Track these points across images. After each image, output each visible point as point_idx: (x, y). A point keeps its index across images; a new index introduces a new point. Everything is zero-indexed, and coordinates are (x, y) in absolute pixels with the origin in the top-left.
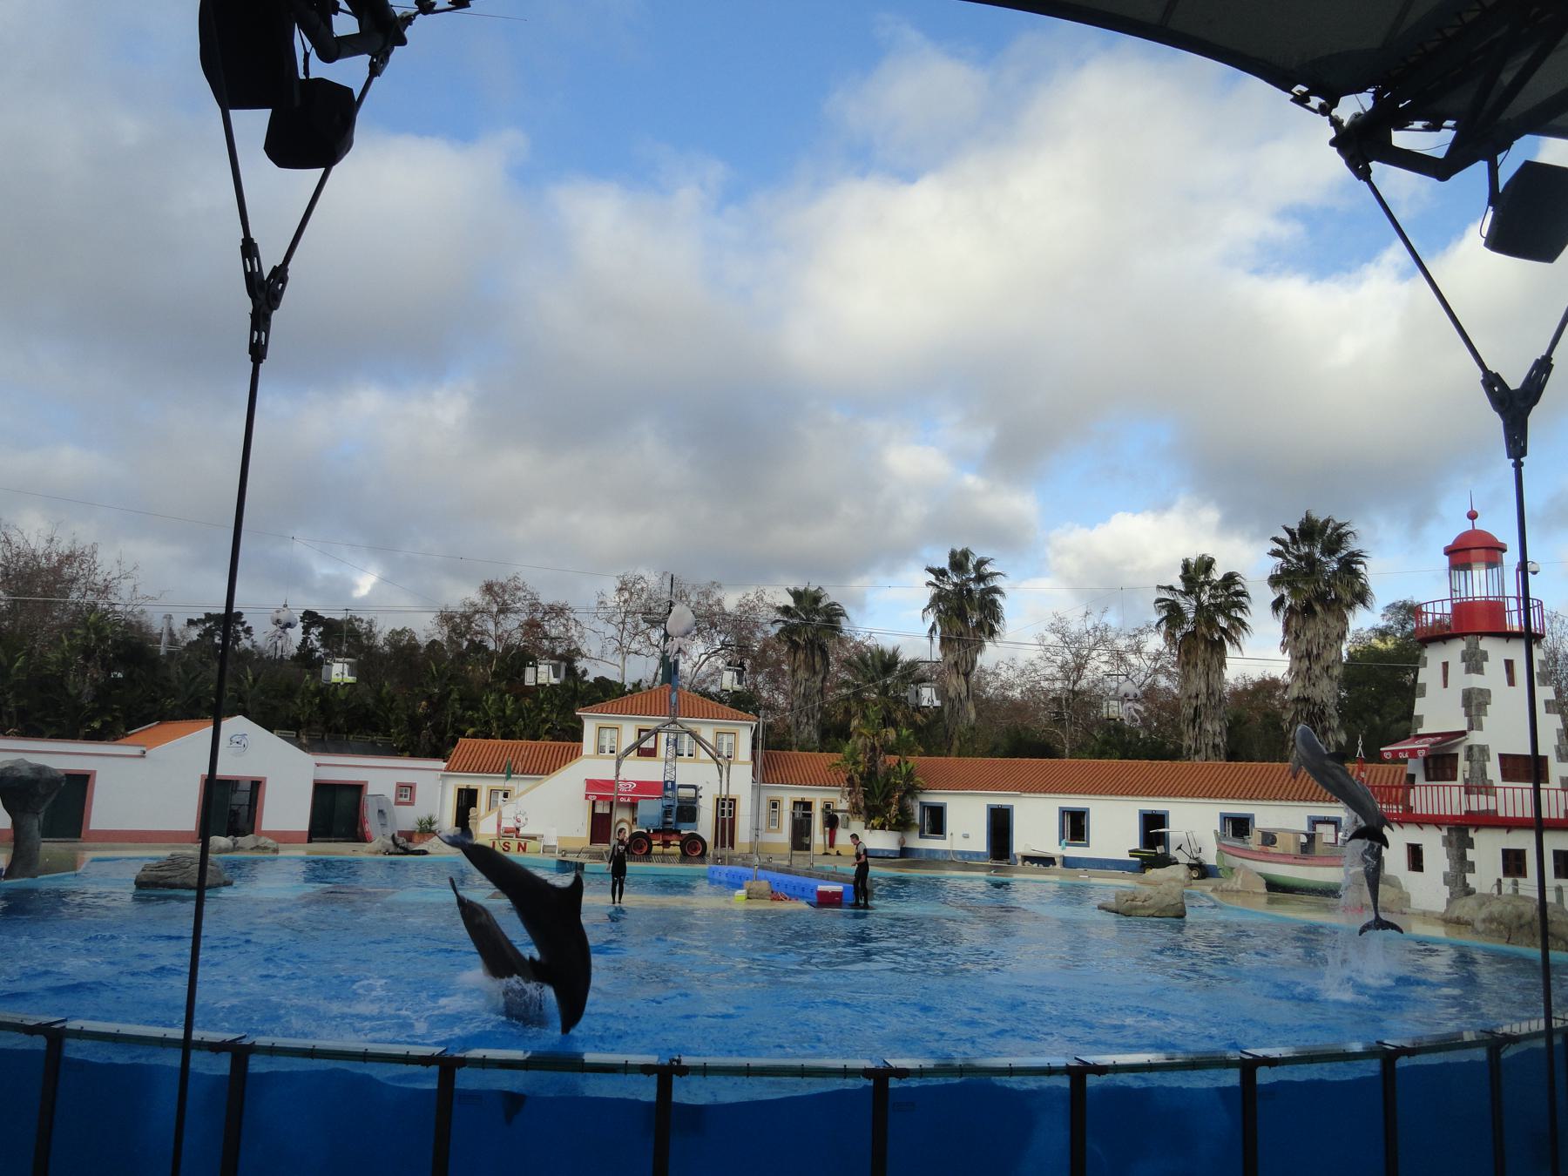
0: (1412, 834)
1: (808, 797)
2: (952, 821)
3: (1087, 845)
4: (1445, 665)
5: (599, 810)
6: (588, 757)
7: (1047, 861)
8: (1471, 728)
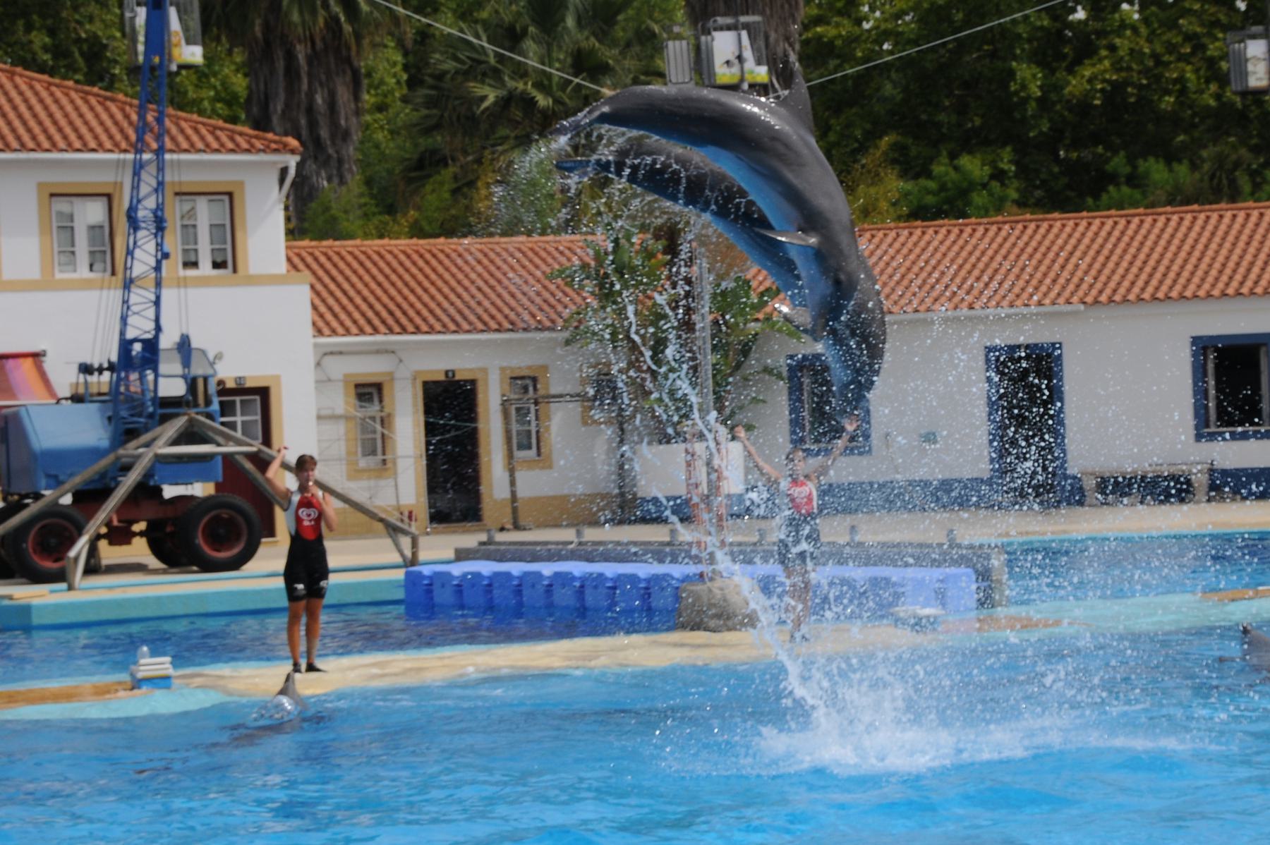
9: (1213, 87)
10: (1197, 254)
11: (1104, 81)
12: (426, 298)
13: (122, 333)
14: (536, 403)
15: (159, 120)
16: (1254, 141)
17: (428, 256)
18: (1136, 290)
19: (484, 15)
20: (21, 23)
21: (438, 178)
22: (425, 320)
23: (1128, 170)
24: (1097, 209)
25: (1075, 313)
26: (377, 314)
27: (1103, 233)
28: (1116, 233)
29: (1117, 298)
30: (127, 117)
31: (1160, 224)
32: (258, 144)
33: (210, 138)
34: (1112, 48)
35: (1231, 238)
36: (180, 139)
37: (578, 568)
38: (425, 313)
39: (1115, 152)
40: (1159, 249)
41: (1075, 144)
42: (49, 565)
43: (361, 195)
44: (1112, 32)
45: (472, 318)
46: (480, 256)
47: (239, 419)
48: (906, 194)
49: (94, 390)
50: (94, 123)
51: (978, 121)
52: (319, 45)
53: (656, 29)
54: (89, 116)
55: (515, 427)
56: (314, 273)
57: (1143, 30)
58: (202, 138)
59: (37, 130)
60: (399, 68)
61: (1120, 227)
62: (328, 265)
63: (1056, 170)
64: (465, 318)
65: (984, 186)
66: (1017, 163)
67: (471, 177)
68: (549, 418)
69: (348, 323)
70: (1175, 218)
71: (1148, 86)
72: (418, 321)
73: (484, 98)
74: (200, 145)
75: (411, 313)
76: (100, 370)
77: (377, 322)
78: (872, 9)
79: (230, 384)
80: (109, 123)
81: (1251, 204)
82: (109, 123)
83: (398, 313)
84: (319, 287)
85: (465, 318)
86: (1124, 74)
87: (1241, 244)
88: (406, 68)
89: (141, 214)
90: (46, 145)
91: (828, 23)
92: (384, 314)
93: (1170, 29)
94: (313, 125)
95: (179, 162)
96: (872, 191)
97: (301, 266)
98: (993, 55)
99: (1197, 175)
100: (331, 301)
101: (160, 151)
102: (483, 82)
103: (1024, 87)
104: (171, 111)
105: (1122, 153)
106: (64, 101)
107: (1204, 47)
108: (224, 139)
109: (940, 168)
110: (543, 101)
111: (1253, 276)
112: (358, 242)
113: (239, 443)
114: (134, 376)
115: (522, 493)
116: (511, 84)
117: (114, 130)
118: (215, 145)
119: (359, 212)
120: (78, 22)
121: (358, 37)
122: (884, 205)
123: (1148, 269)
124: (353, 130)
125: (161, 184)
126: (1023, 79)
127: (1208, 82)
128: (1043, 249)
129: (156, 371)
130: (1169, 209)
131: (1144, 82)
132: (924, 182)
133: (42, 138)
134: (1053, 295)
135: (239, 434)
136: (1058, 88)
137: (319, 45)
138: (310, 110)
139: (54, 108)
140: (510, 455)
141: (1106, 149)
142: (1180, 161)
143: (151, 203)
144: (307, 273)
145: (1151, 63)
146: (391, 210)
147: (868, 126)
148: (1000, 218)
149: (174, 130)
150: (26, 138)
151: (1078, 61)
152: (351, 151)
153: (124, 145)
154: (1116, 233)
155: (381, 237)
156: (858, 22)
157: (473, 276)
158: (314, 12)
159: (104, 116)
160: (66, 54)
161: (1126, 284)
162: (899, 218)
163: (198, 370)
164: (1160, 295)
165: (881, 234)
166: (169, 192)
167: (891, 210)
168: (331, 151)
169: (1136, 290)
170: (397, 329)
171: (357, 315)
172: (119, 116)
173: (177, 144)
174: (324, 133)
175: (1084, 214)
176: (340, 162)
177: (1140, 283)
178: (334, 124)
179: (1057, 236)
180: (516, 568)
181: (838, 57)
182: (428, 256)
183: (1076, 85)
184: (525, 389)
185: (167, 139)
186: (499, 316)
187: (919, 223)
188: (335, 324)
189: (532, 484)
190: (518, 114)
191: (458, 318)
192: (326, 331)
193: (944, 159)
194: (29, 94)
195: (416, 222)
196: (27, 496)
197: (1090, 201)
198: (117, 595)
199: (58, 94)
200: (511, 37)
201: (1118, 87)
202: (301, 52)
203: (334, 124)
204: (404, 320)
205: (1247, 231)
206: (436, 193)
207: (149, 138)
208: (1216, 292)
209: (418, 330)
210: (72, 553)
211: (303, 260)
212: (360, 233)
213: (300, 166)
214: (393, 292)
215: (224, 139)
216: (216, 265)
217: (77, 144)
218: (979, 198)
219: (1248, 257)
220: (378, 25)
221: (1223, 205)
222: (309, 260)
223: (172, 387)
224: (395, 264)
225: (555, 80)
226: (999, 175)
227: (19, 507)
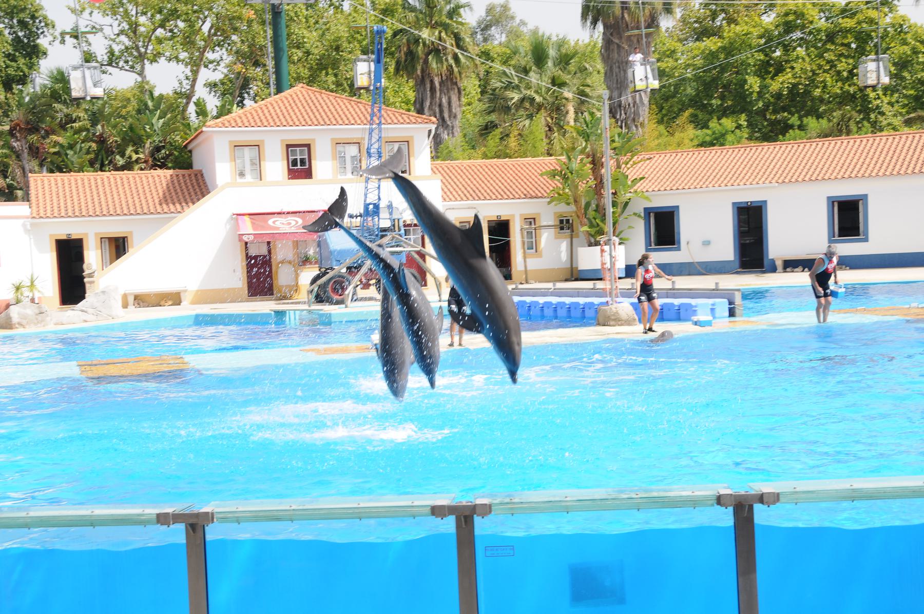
2: (686, 227)
3: (866, 240)
5: (253, 252)
6: (228, 185)
9: (839, 84)
10: (830, 159)
11: (789, 83)
12: (489, 185)
13: (365, 201)
14: (535, 229)
15: (379, 111)
16: (858, 108)
17: (490, 167)
18: (802, 176)
19: (513, 62)
20: (324, 72)
21: (493, 133)
22: (488, 194)
23: (799, 123)
24: (784, 140)
25: (774, 187)
26: (468, 192)
27: (787, 151)
28: (793, 151)
29: (793, 180)
30: (366, 110)
31: (813, 147)
32: (419, 120)
33: (400, 118)
34: (793, 68)
35: (847, 152)
36: (388, 119)
37: (554, 300)
38: (488, 191)
39: (793, 115)
40: (813, 158)
41: (775, 112)
42: (336, 297)
43: (462, 141)
44: (792, 60)
45: (508, 193)
46: (512, 167)
47: (412, 237)
48: (697, 137)
49: (354, 225)
50: (353, 113)
51: (730, 103)
52: (444, 78)
53: (587, 66)
54: (351, 110)
55: (526, 240)
56: (442, 175)
57: (807, 59)
58: (397, 118)
59: (331, 116)
60: (477, 86)
61: (795, 148)
62: (448, 171)
63: (766, 123)
64: (505, 193)
65: (733, 132)
66: (747, 121)
67: (507, 132)
68: (541, 237)
69: (457, 196)
70: (821, 144)
71: (809, 84)
72: (485, 194)
73: (512, 99)
74: (396, 121)
75: (483, 191)
76: (357, 217)
77: (468, 195)
78: (682, 54)
79: (408, 222)
80: (359, 113)
81: (856, 136)
82: (359, 113)
83: (477, 191)
84: (444, 181)
85: (505, 193)
86: (798, 80)
87: (851, 155)
88: (480, 86)
89: (372, 151)
90: (334, 122)
91: (663, 61)
92: (471, 192)
93: (820, 58)
94: (441, 112)
95: (387, 129)
96: (682, 135)
97: (437, 172)
98: (737, 73)
99: (831, 124)
100: (449, 187)
101: (380, 124)
102: (513, 91)
103: (751, 87)
104: (383, 107)
105: (796, 115)
106: (341, 104)
107: (835, 66)
108: (406, 118)
109: (713, 124)
110: (538, 99)
111: (857, 169)
112: (460, 161)
113: (412, 246)
114: (370, 219)
115: (529, 268)
116: (524, 92)
117: (361, 116)
118: (402, 121)
119: (461, 149)
120: (347, 71)
121: (460, 73)
122: (687, 141)
123: (807, 167)
124: (458, 114)
125: (380, 137)
126: (751, 83)
127: (837, 82)
128: (759, 159)
129: (378, 216)
130: (818, 139)
131: (807, 83)
132: (705, 131)
133: (333, 120)
134: (763, 179)
135: (412, 243)
136: (766, 87)
137: (444, 78)
138: (440, 106)
139: (337, 107)
140: (524, 253)
141: (788, 114)
142: (823, 118)
143: (376, 146)
144: (439, 175)
145: (810, 74)
146: (473, 148)
147: (680, 107)
148: (740, 146)
149: (385, 115)
150: (326, 120)
151: (776, 75)
152: (457, 123)
153: (365, 122)
154: (793, 151)
155: (470, 159)
156: (676, 60)
157: (509, 175)
158: (442, 62)
159: (357, 110)
160: (341, 85)
161: (797, 174)
162: (694, 146)
163: (395, 216)
164: (813, 178)
165: (685, 154)
166: (383, 141)
167: (690, 143)
168: (449, 123)
169: (802, 176)
170: (477, 198)
171: (460, 193)
172: (363, 110)
173: (386, 121)
174: (446, 115)
175: (778, 143)
176: (453, 127)
177: (804, 173)
178: (450, 110)
179: (766, 153)
180: (528, 299)
181: (667, 76)
182: (490, 167)
183: (775, 86)
184: (531, 223)
185: (382, 119)
186: (520, 193)
187: (703, 148)
188: (451, 196)
189: (534, 264)
190: (527, 105)
191: (502, 193)
192: (447, 199)
193: (715, 120)
194: (327, 101)
195: (485, 152)
196: (327, 269)
197: (781, 137)
198: (365, 310)
199: (339, 101)
200: (526, 71)
201: (795, 86)
202: (437, 81)
203: (450, 110)
204: (480, 195)
205: (854, 149)
206: (493, 139)
207: (375, 118)
208: (839, 177)
209: (485, 199)
210: (347, 292)
211: (437, 169)
212: (461, 157)
213: (437, 129)
214: (475, 182)
215: (406, 118)
217: (347, 122)
218: (730, 137)
219: (855, 161)
220: (468, 68)
221: (843, 137)
222: (440, 169)
223: (386, 224)
224: (476, 171)
225: (543, 89)
226: (739, 127)
227: (325, 273)
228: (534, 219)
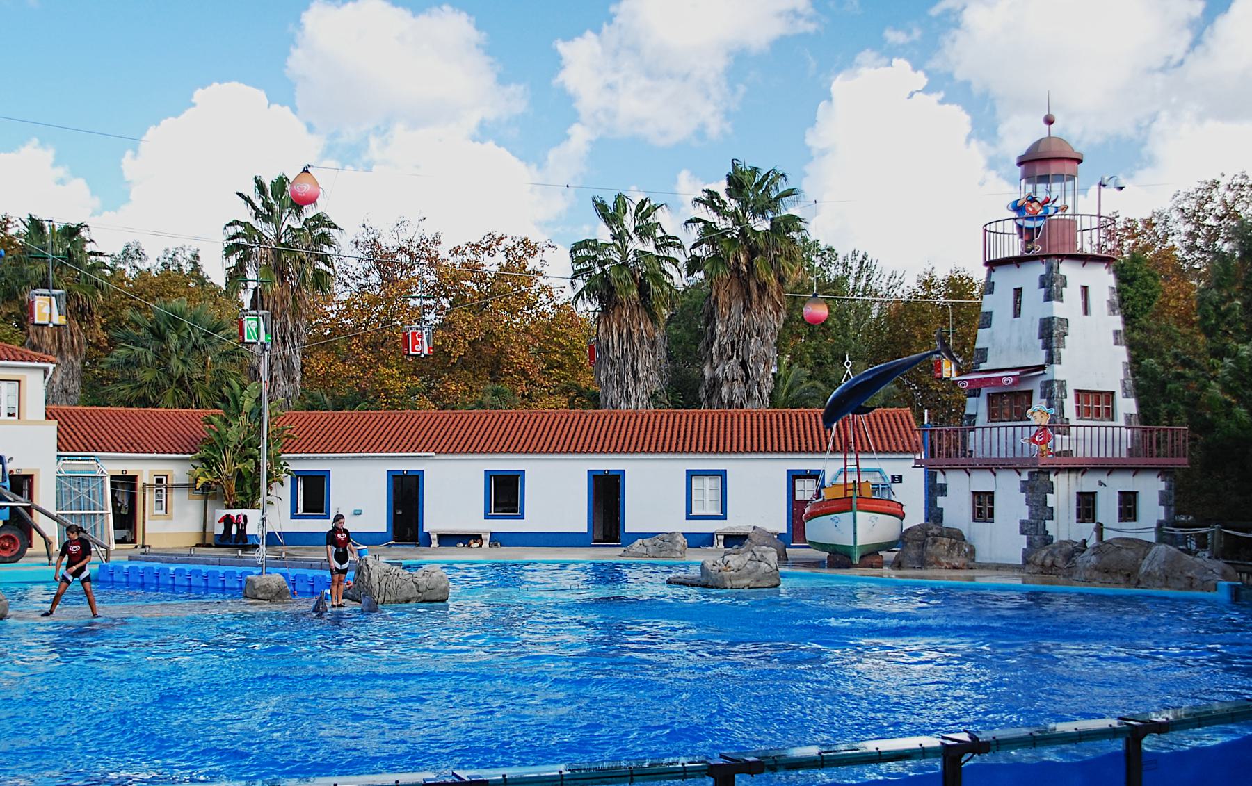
0: (983, 482)
1: (131, 469)
4: (1018, 292)
7: (468, 539)
8: (1050, 360)
216: (9, 415)
228: (166, 476)
